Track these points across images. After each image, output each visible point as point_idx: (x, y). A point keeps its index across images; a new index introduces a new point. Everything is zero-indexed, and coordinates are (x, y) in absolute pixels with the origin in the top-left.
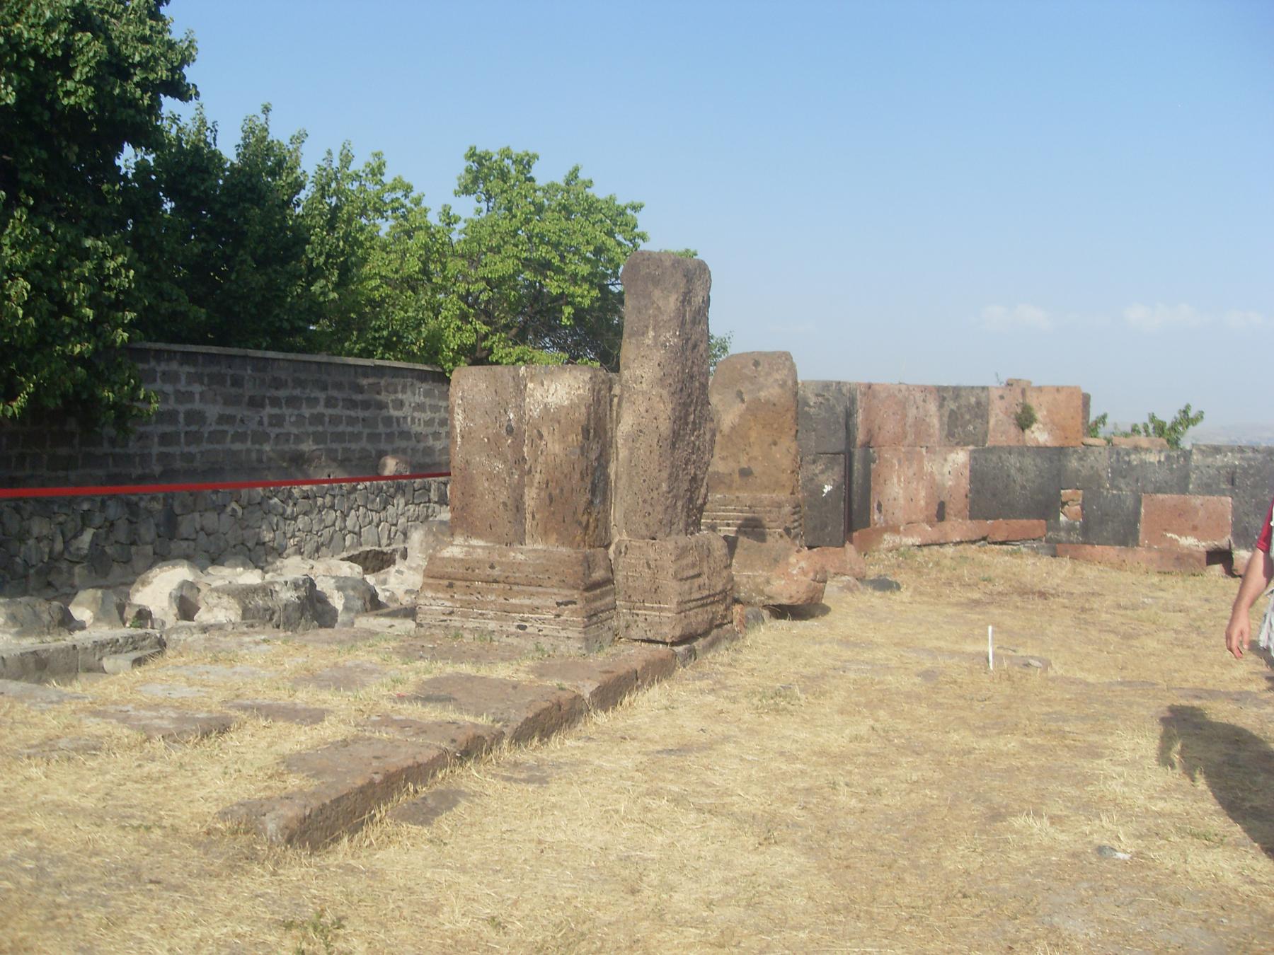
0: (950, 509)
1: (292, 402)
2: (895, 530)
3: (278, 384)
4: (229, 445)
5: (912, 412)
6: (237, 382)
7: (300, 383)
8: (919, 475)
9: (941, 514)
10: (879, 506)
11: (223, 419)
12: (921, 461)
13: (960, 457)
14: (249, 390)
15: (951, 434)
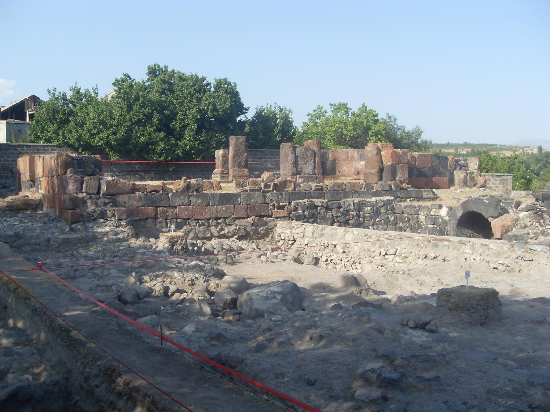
0: (361, 173)
1: (269, 158)
2: (345, 176)
3: (266, 155)
4: (254, 165)
5: (350, 154)
6: (255, 155)
7: (271, 155)
8: (352, 166)
9: (358, 173)
10: (339, 172)
11: (252, 161)
12: (352, 163)
13: (363, 163)
14: (258, 156)
15: (360, 158)
